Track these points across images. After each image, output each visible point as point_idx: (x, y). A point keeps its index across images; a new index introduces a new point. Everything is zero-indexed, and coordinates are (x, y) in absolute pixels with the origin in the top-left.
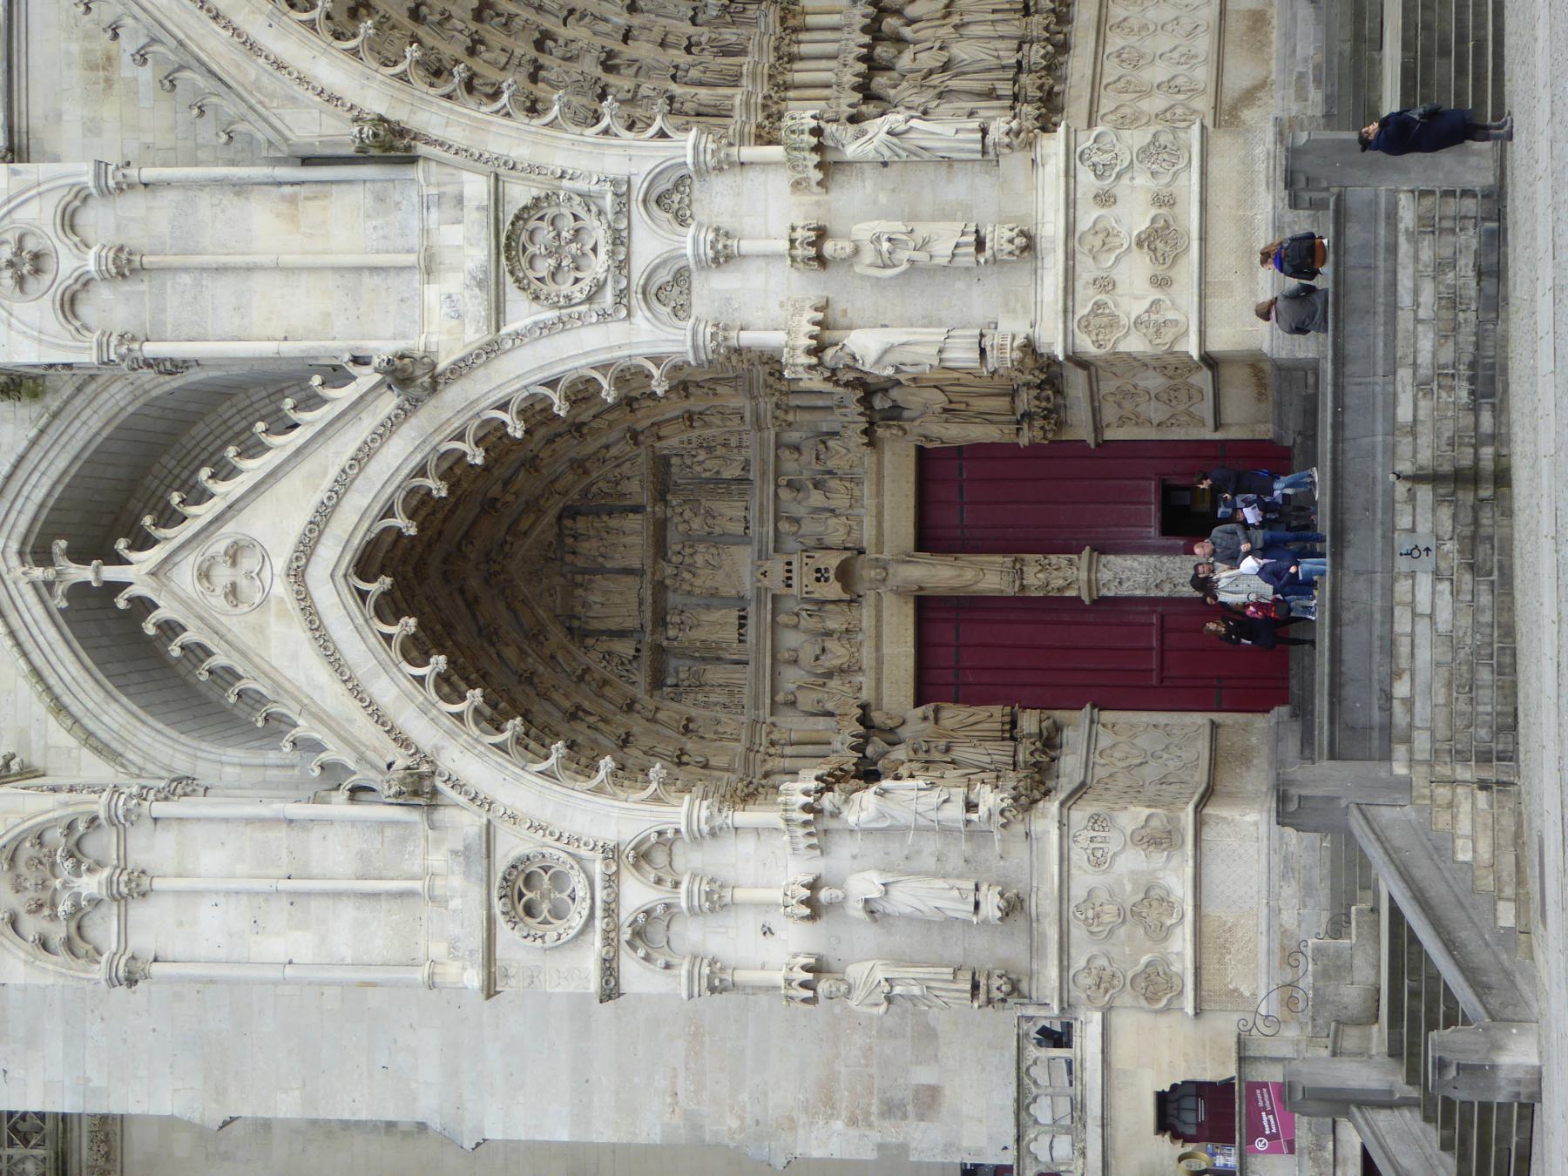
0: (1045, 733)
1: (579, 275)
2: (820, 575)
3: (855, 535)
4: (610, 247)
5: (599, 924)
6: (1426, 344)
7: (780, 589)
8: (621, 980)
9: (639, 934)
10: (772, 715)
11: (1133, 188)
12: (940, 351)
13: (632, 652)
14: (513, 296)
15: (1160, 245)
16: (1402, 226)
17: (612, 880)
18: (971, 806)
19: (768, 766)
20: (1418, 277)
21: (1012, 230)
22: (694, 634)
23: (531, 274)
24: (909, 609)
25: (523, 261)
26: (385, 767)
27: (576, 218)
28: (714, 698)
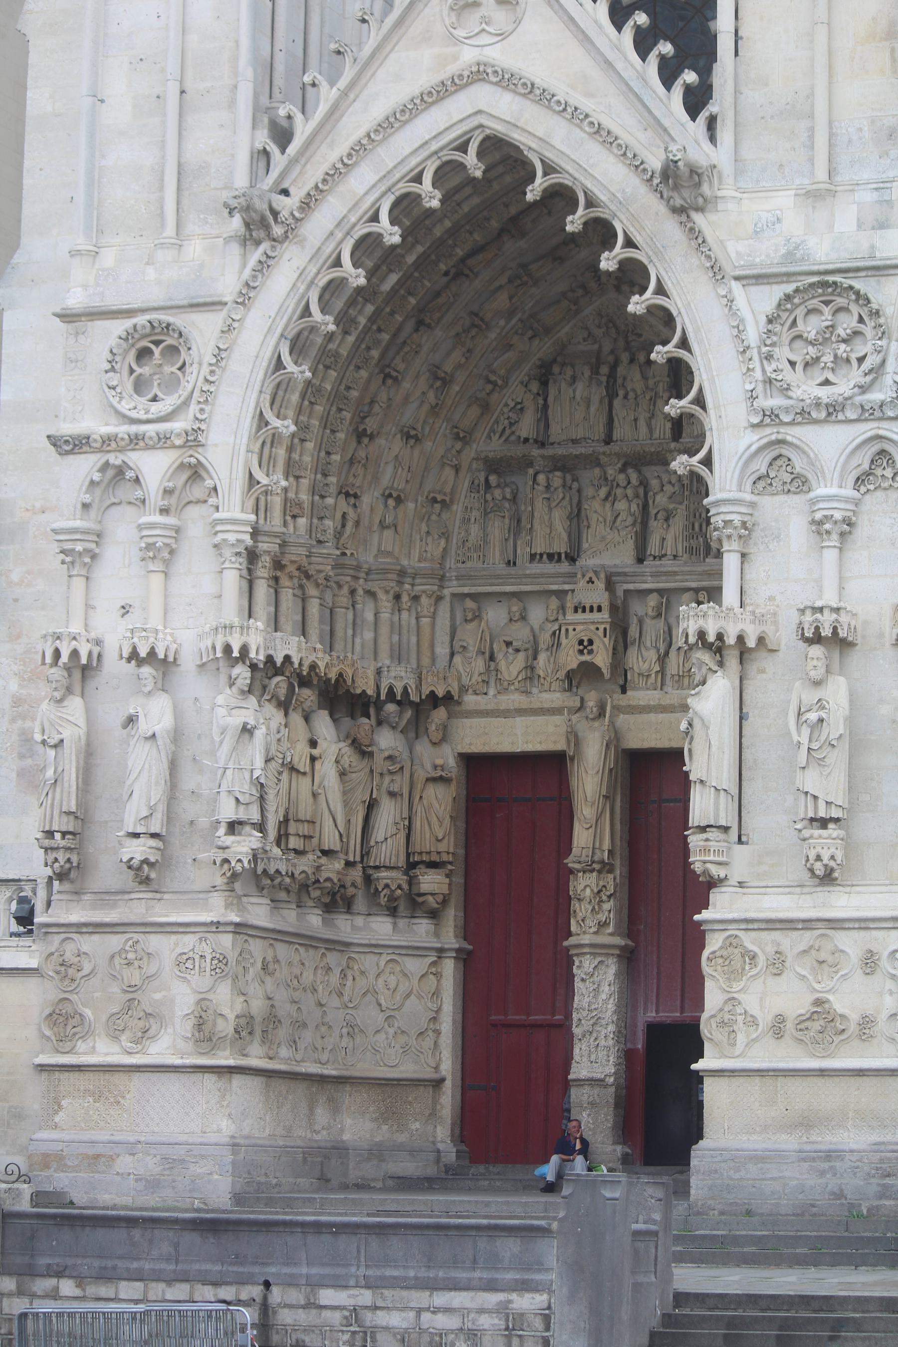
0: (420, 900)
1: (799, 367)
2: (586, 645)
3: (642, 682)
4: (825, 400)
5: (123, 430)
6: (396, 1320)
7: (570, 605)
8: (72, 456)
9: (120, 471)
10: (454, 595)
11: (881, 994)
12: (702, 781)
13: (524, 434)
14: (778, 291)
15: (817, 1025)
16: (514, 1296)
17: (163, 441)
18: (233, 827)
19: (381, 595)
20: (463, 1312)
21: (832, 857)
22: (539, 504)
23: (800, 312)
24: (560, 746)
25: (815, 301)
26: (285, 185)
27: (861, 360)
28: (475, 530)
